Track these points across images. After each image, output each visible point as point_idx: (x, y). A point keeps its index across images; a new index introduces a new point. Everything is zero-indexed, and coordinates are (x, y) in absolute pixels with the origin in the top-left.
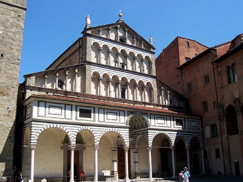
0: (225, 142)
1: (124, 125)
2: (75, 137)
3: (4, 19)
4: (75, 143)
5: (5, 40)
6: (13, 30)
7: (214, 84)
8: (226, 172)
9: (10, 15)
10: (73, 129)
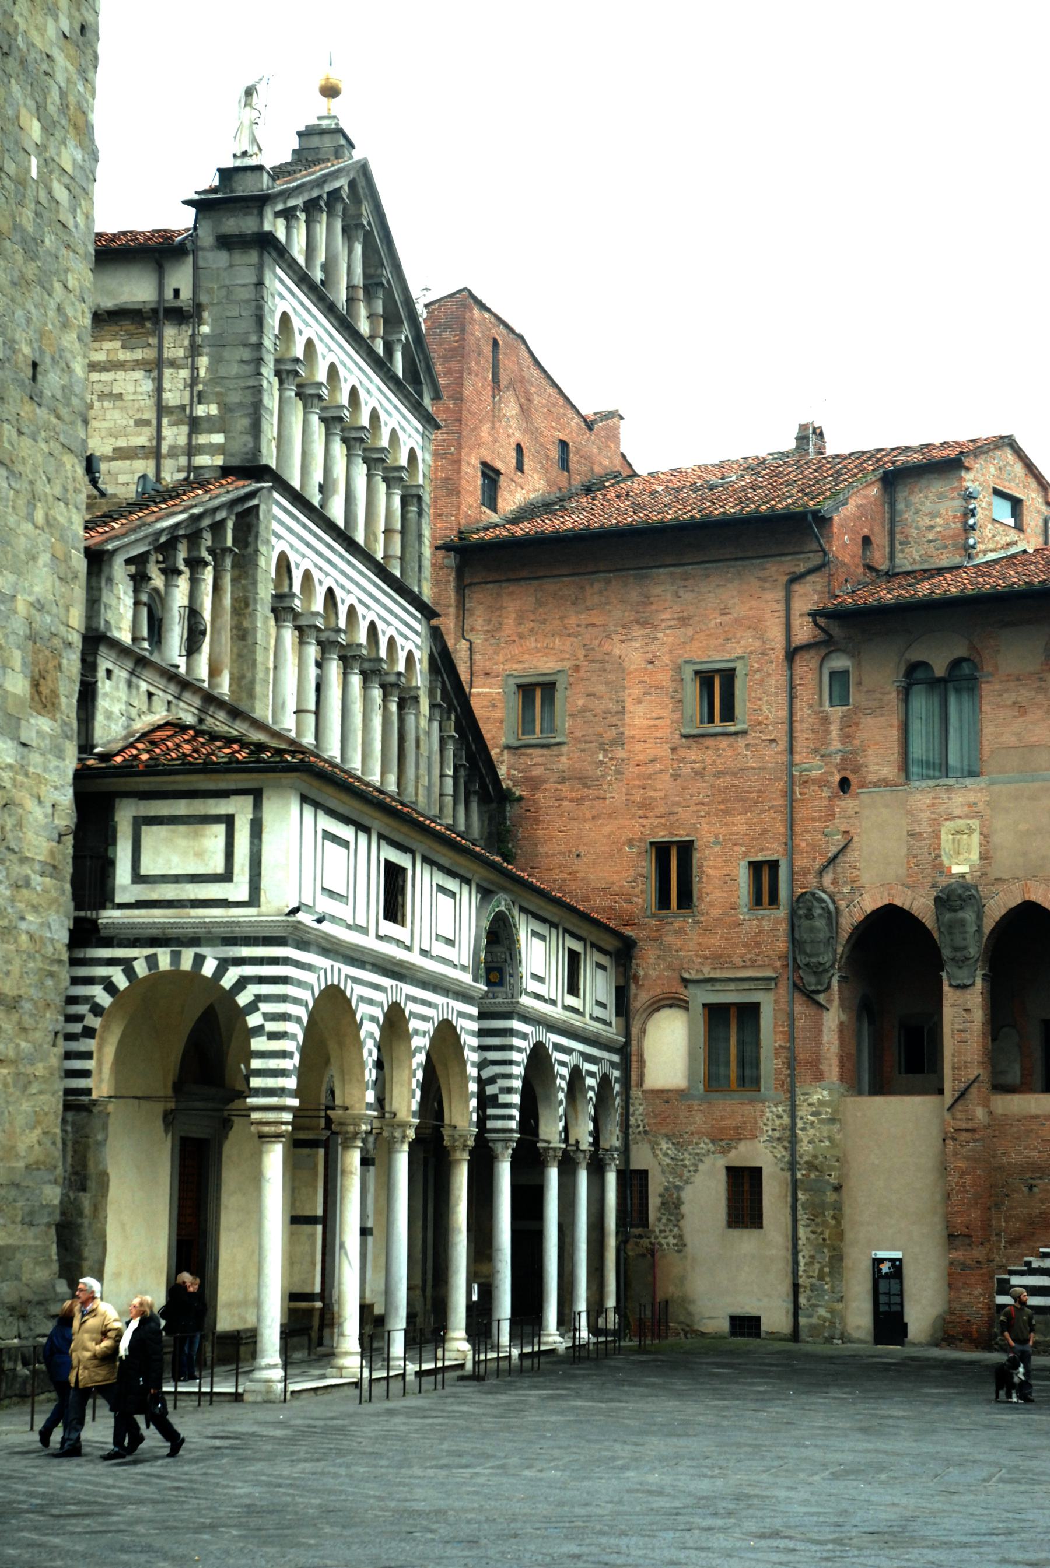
0: (811, 1132)
1: (467, 978)
7: (783, 744)
8: (803, 1321)
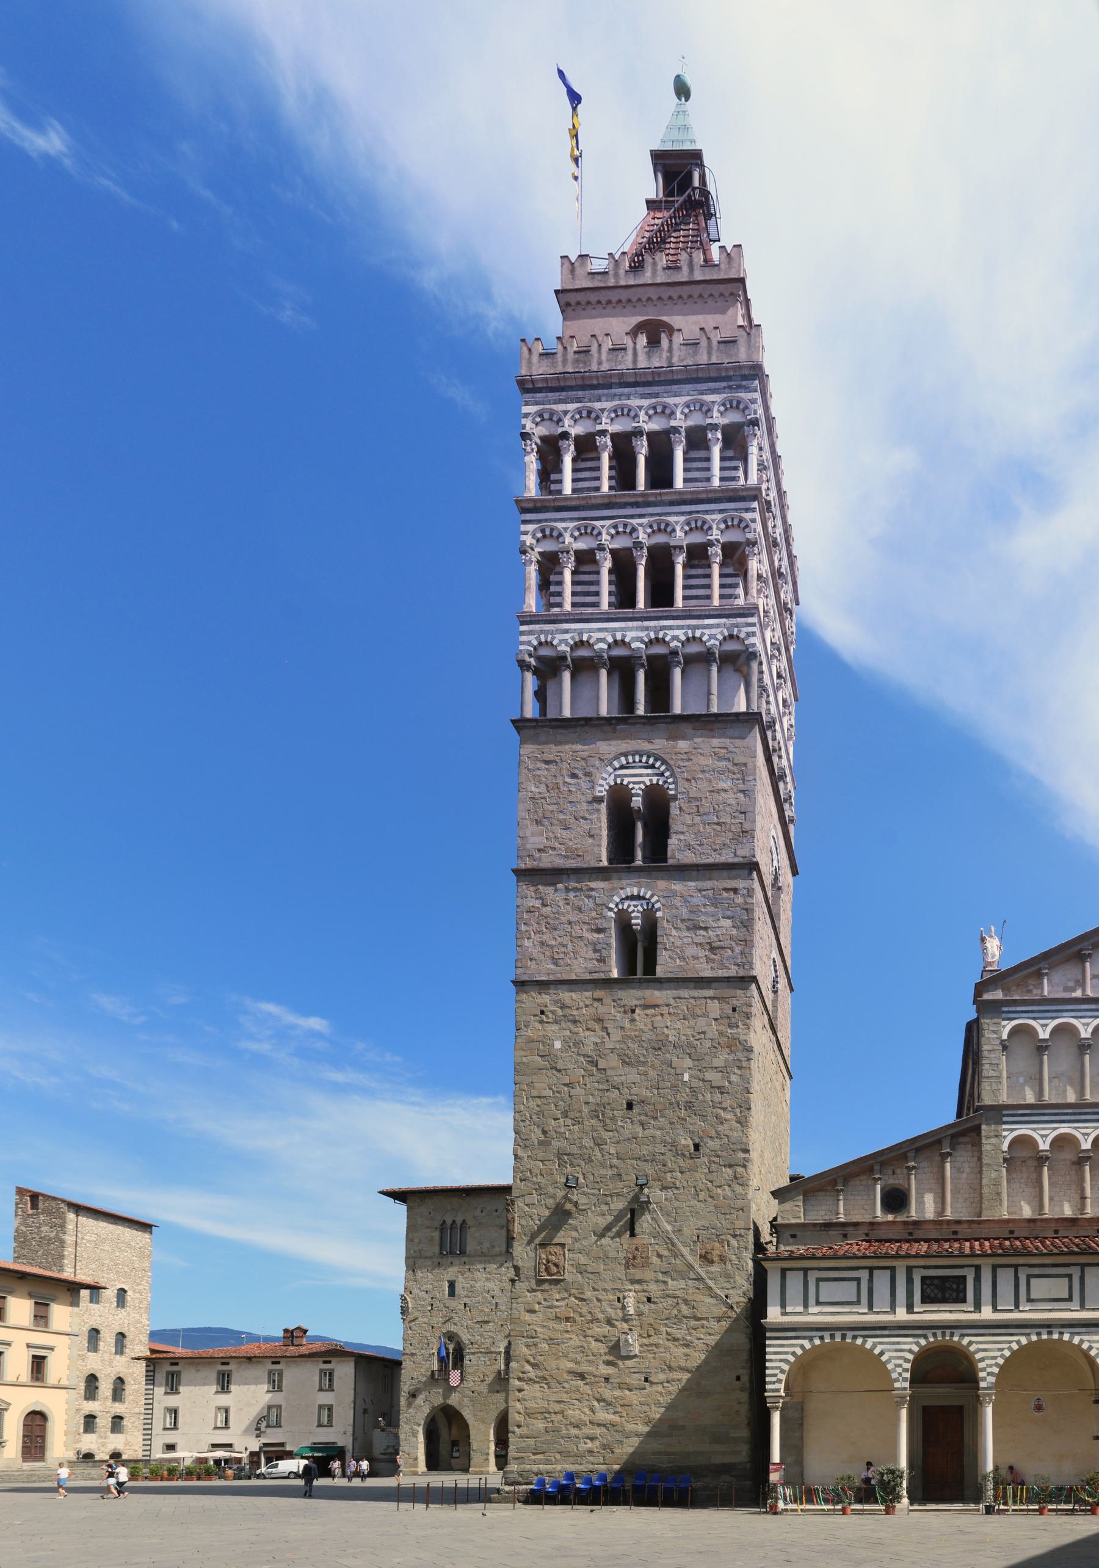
2: (908, 1366)
3: (689, 1032)
4: (907, 1385)
5: (700, 1097)
6: (719, 1062)
9: (705, 1015)
10: (898, 1343)
